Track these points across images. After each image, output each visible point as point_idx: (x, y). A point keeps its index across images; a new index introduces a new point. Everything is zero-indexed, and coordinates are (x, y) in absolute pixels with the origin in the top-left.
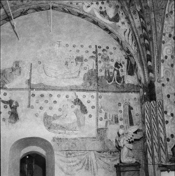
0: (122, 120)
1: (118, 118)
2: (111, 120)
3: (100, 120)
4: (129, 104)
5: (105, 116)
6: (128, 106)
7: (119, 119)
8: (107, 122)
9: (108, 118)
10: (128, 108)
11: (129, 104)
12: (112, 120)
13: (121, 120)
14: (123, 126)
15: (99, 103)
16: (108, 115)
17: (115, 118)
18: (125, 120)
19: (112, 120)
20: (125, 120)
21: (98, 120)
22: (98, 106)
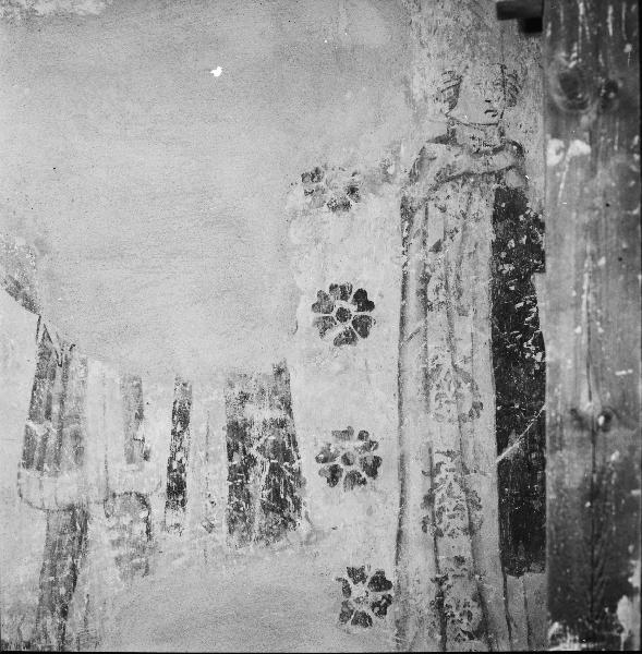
0: (373, 468)
1: (284, 451)
2: (153, 478)
4: (501, 161)
5: (40, 410)
6: (483, 207)
7: (307, 462)
8: (76, 519)
9: (92, 448)
10: (485, 232)
11: (501, 161)
12: (176, 490)
13: (355, 468)
14: (380, 582)
16: (96, 386)
17: (237, 431)
18: (415, 469)
19: (176, 490)
20: (415, 469)
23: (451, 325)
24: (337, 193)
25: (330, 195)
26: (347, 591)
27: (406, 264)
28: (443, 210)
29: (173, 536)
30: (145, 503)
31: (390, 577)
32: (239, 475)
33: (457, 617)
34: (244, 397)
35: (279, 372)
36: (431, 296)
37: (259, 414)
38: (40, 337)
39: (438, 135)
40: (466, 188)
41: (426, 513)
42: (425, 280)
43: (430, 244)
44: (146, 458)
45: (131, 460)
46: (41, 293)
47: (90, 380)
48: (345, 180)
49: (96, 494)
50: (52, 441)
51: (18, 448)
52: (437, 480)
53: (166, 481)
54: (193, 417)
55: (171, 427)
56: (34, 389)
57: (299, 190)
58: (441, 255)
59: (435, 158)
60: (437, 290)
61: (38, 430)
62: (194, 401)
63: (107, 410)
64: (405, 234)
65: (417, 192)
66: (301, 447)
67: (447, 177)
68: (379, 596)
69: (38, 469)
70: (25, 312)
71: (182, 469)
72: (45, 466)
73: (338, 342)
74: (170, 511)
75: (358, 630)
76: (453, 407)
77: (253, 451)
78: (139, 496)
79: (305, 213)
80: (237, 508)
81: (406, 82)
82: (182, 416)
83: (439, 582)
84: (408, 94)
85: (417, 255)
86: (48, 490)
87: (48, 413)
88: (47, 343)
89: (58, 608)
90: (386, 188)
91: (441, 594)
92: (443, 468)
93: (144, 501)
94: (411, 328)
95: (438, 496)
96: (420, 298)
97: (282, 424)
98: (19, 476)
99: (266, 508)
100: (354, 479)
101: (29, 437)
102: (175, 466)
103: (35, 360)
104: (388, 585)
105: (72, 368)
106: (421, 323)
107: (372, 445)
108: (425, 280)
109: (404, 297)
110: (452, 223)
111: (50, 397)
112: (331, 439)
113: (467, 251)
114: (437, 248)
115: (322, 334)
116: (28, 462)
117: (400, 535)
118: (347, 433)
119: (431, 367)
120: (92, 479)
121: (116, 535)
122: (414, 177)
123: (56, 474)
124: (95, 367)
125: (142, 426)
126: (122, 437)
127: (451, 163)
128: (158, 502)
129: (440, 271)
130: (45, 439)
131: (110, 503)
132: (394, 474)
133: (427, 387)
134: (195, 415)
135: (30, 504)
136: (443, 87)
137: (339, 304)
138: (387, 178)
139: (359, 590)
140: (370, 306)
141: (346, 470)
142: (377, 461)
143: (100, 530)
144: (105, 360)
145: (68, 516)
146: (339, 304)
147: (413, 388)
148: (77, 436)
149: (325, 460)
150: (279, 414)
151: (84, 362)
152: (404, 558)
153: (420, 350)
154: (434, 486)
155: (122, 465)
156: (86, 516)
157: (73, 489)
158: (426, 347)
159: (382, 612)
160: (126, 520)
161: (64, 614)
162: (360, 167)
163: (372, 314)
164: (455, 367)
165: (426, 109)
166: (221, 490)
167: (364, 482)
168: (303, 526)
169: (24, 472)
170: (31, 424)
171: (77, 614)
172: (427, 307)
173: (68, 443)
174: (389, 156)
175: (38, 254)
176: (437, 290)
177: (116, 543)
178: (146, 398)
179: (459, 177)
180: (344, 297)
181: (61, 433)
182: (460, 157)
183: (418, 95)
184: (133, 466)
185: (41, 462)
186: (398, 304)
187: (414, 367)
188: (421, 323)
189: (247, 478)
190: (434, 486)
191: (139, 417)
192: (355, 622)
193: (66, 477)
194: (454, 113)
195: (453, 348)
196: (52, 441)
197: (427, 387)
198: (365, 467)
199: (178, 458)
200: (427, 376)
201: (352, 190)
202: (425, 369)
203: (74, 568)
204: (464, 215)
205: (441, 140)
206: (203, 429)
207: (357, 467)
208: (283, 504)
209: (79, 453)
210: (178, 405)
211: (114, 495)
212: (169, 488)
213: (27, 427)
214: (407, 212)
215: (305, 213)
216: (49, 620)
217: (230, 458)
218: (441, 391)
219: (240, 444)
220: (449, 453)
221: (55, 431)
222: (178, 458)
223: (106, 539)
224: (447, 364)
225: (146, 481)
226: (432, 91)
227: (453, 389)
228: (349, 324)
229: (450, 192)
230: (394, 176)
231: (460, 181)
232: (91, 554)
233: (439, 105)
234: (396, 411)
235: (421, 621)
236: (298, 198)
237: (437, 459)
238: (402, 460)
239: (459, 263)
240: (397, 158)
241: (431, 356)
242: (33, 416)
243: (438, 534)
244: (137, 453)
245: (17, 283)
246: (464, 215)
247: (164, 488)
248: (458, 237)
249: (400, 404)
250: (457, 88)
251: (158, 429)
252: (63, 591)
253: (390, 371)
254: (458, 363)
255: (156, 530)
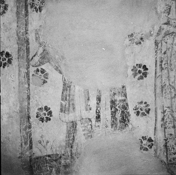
0: (148, 111)
1: (125, 107)
2: (92, 115)
3: (42, 120)
5: (64, 98)
7: (131, 110)
8: (74, 125)
9: (77, 107)
12: (98, 117)
13: (143, 111)
14: (150, 140)
15: (31, 37)
16: (77, 91)
17: (113, 102)
19: (98, 117)
20: (159, 111)
21: (29, 117)
22: (28, 49)
23: (169, 74)
24: (137, 40)
25: (136, 40)
26: (142, 142)
27: (156, 58)
28: (166, 43)
29: (97, 129)
30: (90, 121)
31: (153, 139)
32: (113, 114)
33: (170, 149)
34: (115, 94)
35: (123, 87)
36: (163, 66)
37: (118, 98)
38: (63, 81)
39: (164, 23)
40: (172, 37)
41: (162, 123)
42: (162, 62)
43: (163, 52)
44: (90, 109)
45: (87, 110)
46: (63, 69)
47: (76, 91)
48: (139, 36)
49: (78, 118)
50: (67, 106)
51: (59, 108)
52: (165, 114)
53: (95, 115)
54: (102, 99)
55: (96, 102)
56: (62, 93)
57: (127, 40)
58: (166, 55)
59: (164, 29)
60: (165, 64)
61: (64, 103)
62: (102, 95)
63: (80, 98)
64: (156, 50)
65: (159, 38)
66: (129, 106)
67: (167, 34)
68: (150, 143)
69: (64, 112)
70: (60, 74)
71: (99, 112)
72: (66, 112)
73: (139, 79)
74: (97, 122)
75: (145, 152)
76: (169, 95)
77: (117, 107)
78: (89, 119)
79: (129, 45)
80: (113, 122)
81: (156, 8)
82: (99, 99)
83: (166, 140)
84: (157, 12)
85: (159, 55)
86: (67, 118)
87: (66, 99)
88: (65, 82)
89: (70, 146)
90: (151, 38)
91: (166, 143)
92: (167, 111)
93: (90, 120)
94: (158, 75)
95: (165, 118)
96: (160, 67)
97: (125, 100)
98: (60, 114)
99: (120, 122)
100: (143, 114)
101: (61, 105)
102: (98, 111)
103: (62, 86)
104: (152, 141)
105: (71, 88)
106: (160, 73)
107: (148, 105)
108: (162, 62)
109: (156, 67)
110: (169, 46)
111: (66, 95)
112: (137, 104)
113: (173, 54)
114: (165, 53)
115: (134, 77)
116: (61, 110)
117: (155, 128)
118: (141, 103)
119: (163, 85)
120: (77, 115)
121: (84, 128)
122: (158, 34)
123: (69, 114)
124: (77, 88)
125: (89, 102)
126: (84, 104)
127: (168, 30)
128: (94, 121)
129: (166, 59)
130: (65, 105)
131: (82, 120)
132: (154, 113)
133: (162, 90)
134: (102, 99)
135: (63, 121)
136: (166, 9)
137: (139, 69)
138: (151, 35)
139: (145, 142)
140: (147, 69)
141: (141, 112)
142: (149, 110)
143: (79, 127)
144: (79, 85)
145: (72, 123)
146: (139, 69)
147: (158, 90)
148: (73, 104)
149: (136, 110)
150: (123, 98)
151: (74, 86)
152: (156, 134)
153: (160, 81)
154: (164, 116)
155: (84, 111)
156: (76, 124)
157: (73, 117)
158: (162, 79)
159: (151, 147)
160: (86, 125)
161: (72, 147)
162: (144, 32)
163: (148, 71)
164: (170, 84)
165: (161, 15)
166: (109, 117)
167: (146, 115)
168: (130, 126)
169: (60, 113)
170: (62, 102)
171: (75, 147)
172: (162, 69)
173: (71, 106)
174: (151, 29)
175: (62, 59)
176: (165, 64)
177: (84, 130)
178: (90, 95)
179: (170, 33)
180: (140, 67)
181: (69, 104)
182: (171, 28)
183: (159, 12)
184: (87, 112)
185: (65, 111)
186: (154, 68)
187: (159, 85)
188: (160, 73)
189: (116, 114)
190: (164, 116)
191: (88, 99)
192: (144, 150)
193: (71, 114)
194: (169, 16)
195: (169, 80)
196: (67, 106)
197: (162, 90)
198: (146, 111)
199: (98, 109)
200: (162, 87)
201: (142, 39)
202: (162, 85)
203: (74, 136)
204: (172, 44)
205: (166, 24)
206: (104, 102)
207: (144, 111)
208: (125, 121)
209: (74, 108)
210: (98, 96)
211: (83, 119)
212: (96, 117)
213: (61, 102)
214: (156, 44)
215: (129, 45)
216: (68, 149)
217: (111, 109)
218: (166, 91)
219: (114, 106)
220: (168, 107)
221: (68, 103)
222: (98, 109)
223: (81, 129)
224: (168, 84)
225: (90, 115)
226: (163, 10)
227: (169, 90)
228: (141, 74)
229: (168, 38)
230: (153, 34)
231: (171, 35)
232: (78, 133)
233: (165, 14)
234: (154, 96)
235: (161, 150)
236: (127, 41)
237: (165, 109)
238: (156, 108)
239: (171, 57)
240: (154, 29)
241: (163, 82)
242: (62, 100)
243: (165, 128)
244: (88, 108)
245: (57, 67)
246: (172, 44)
247: (95, 117)
248: (170, 50)
249: (155, 95)
250: (170, 9)
251: (93, 102)
252: (71, 142)
253: (152, 86)
254: (171, 84)
255: (93, 127)
